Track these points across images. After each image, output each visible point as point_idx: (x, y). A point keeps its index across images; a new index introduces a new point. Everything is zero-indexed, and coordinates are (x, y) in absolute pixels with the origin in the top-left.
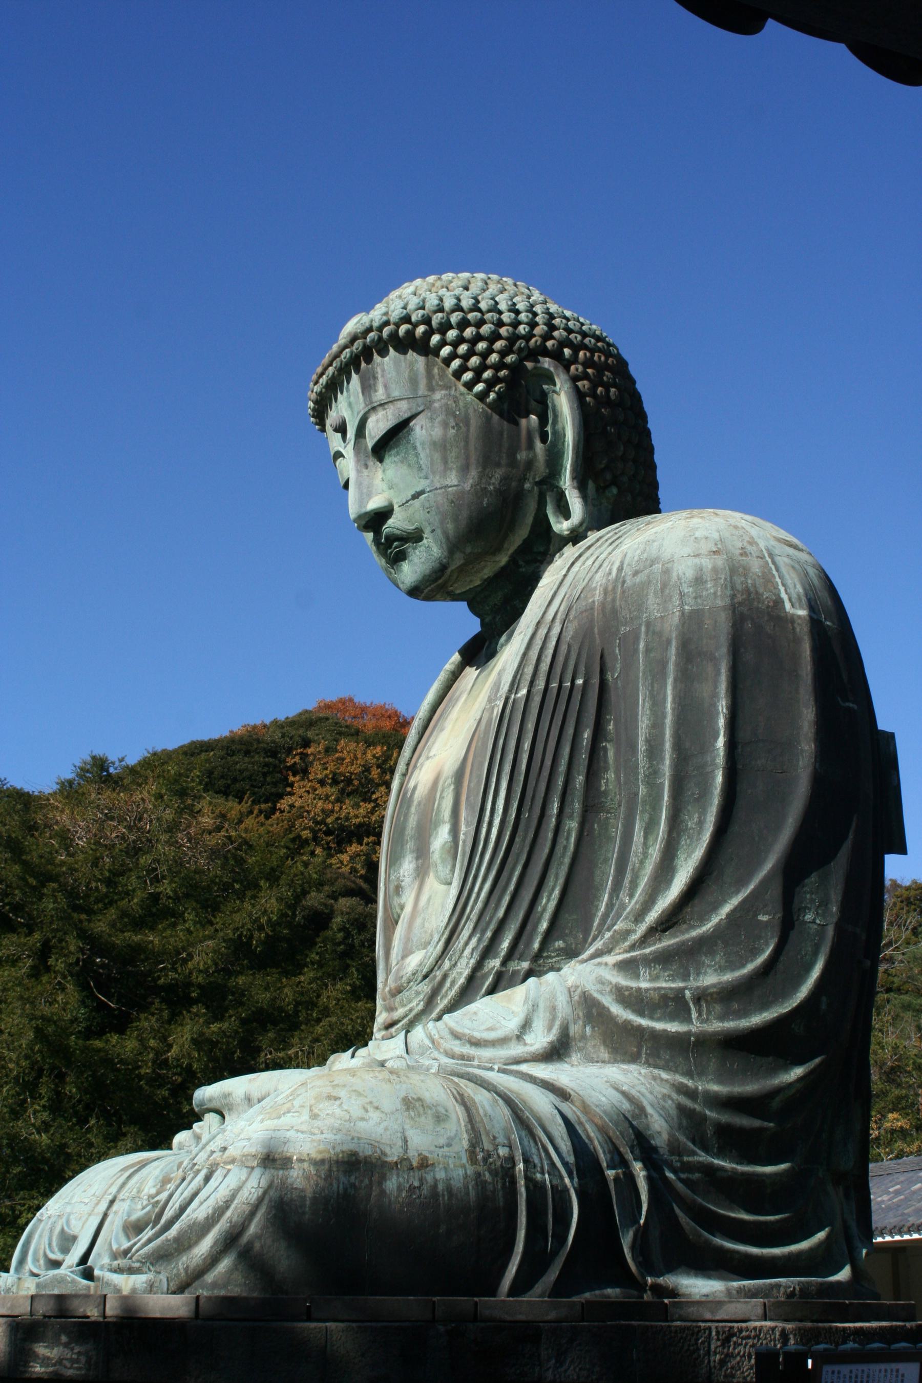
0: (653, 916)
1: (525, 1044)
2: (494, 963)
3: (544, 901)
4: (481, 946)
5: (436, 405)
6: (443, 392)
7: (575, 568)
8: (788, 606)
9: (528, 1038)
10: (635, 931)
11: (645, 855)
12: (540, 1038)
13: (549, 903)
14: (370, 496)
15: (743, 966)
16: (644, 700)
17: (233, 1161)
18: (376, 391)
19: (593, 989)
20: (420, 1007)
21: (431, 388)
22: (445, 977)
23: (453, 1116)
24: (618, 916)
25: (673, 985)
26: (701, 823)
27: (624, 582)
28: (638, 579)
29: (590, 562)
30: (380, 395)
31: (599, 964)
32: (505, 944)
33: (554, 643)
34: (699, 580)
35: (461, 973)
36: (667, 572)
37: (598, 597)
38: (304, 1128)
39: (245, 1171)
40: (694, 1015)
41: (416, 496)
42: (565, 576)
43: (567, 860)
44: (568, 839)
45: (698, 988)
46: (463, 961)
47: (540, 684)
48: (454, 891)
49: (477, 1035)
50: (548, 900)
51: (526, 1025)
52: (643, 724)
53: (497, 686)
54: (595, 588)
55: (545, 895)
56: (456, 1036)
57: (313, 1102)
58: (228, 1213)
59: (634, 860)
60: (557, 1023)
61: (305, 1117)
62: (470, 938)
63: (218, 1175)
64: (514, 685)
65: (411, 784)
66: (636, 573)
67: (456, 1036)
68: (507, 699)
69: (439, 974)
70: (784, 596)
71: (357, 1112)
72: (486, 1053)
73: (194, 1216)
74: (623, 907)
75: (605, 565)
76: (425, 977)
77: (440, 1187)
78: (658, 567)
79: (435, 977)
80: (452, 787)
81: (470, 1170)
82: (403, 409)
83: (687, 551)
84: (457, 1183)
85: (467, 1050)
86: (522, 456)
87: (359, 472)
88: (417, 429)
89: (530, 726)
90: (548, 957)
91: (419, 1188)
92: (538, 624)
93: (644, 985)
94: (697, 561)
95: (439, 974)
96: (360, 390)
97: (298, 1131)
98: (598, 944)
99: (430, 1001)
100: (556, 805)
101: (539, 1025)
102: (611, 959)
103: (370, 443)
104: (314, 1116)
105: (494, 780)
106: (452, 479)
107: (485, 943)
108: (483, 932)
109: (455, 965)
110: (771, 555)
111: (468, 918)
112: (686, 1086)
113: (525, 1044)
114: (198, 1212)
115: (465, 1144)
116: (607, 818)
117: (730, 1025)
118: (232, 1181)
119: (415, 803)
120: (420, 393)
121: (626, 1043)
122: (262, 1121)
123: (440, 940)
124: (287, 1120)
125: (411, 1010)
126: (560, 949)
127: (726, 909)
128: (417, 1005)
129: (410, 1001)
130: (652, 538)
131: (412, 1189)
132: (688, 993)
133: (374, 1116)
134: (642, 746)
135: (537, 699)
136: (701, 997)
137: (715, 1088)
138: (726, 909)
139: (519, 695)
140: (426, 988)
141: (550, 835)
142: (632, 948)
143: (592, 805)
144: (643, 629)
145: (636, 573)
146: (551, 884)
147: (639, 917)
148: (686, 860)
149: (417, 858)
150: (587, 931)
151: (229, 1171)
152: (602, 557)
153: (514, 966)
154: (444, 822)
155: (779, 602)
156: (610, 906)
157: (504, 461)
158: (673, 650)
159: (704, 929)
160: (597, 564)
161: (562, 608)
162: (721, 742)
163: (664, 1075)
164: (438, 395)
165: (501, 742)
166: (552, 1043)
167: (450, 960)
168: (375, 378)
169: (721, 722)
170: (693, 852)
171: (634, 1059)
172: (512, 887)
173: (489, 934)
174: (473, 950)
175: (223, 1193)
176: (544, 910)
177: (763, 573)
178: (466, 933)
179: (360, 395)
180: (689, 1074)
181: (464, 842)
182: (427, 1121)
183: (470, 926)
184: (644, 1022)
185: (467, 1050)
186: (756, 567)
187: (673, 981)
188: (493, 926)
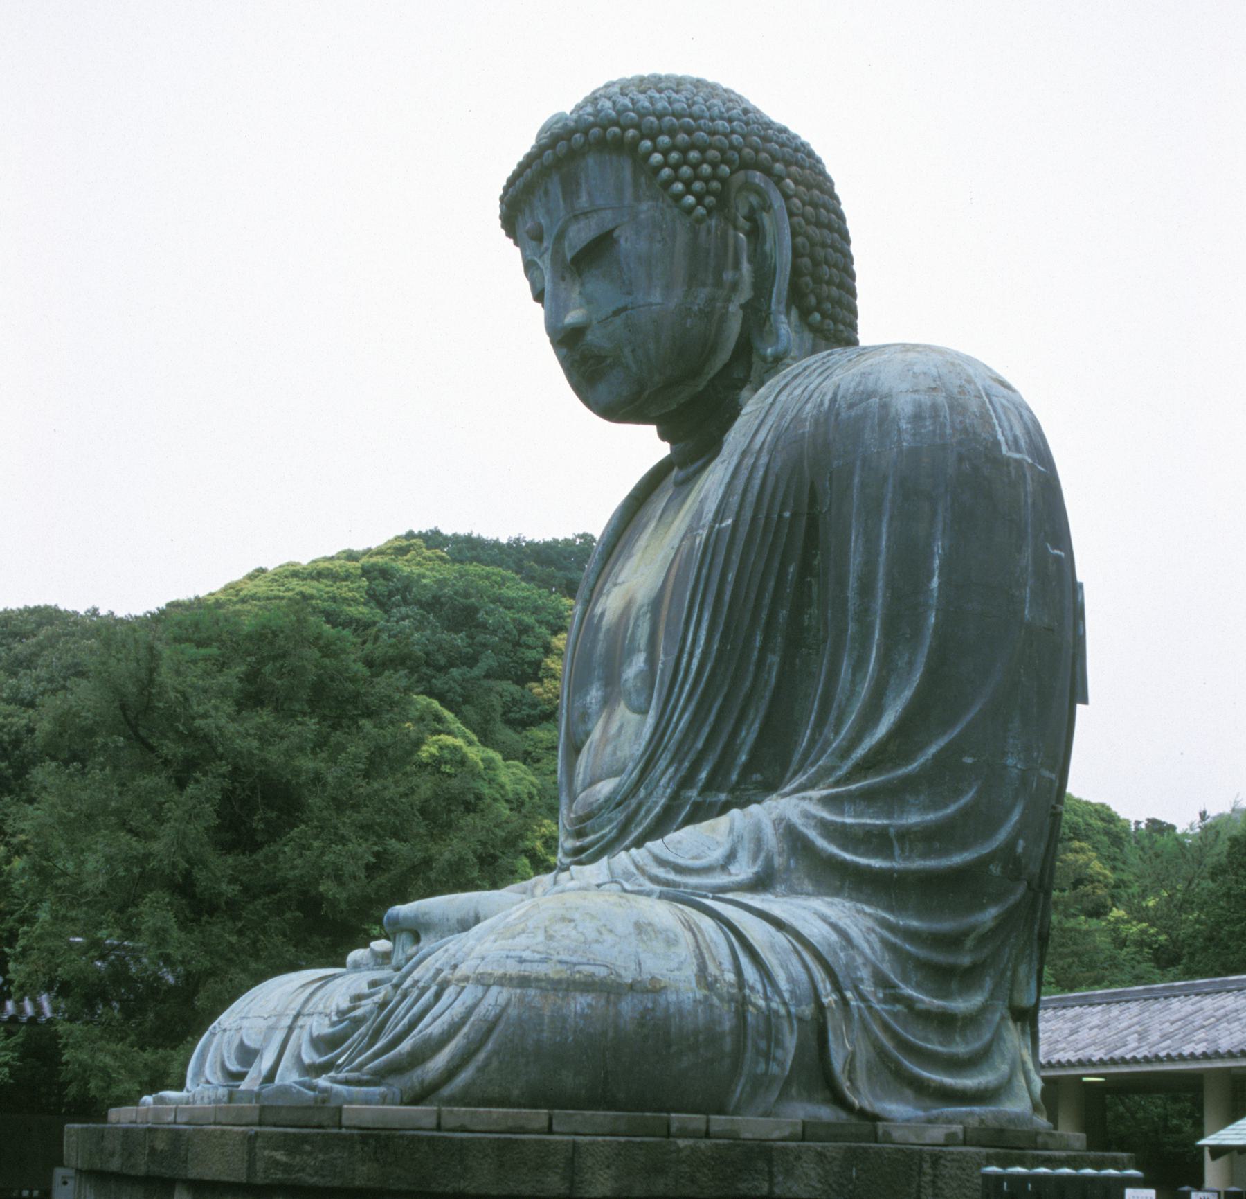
0: (859, 753)
1: (730, 874)
2: (693, 794)
3: (743, 734)
5: (642, 216)
6: (650, 203)
7: (783, 397)
8: (1004, 448)
10: (840, 767)
11: (853, 693)
12: (743, 870)
13: (749, 735)
14: (567, 310)
15: (946, 806)
16: (857, 537)
17: (467, 979)
18: (579, 198)
19: (798, 821)
20: (613, 834)
21: (637, 198)
22: (640, 805)
23: (682, 940)
24: (823, 751)
25: (878, 822)
26: (911, 663)
27: (838, 414)
28: (853, 413)
29: (798, 392)
30: (583, 201)
31: (804, 798)
32: (703, 775)
33: (761, 473)
34: (917, 417)
35: (656, 803)
36: (884, 406)
37: (808, 427)
38: (540, 948)
39: (480, 989)
40: (897, 852)
41: (616, 313)
42: (772, 404)
43: (768, 694)
44: (769, 672)
45: (902, 826)
46: (660, 791)
47: (748, 514)
48: (651, 719)
49: (681, 861)
50: (748, 734)
51: (731, 857)
52: (855, 562)
53: (698, 515)
54: (806, 419)
55: (745, 728)
56: (661, 862)
57: (547, 923)
58: (465, 1029)
59: (840, 695)
60: (762, 855)
61: (541, 937)
62: (667, 768)
63: (450, 991)
64: (719, 515)
65: (598, 610)
66: (851, 406)
67: (661, 862)
68: (712, 528)
69: (634, 803)
70: (1000, 437)
71: (592, 935)
72: (693, 880)
73: (429, 1031)
74: (828, 743)
75: (815, 395)
76: (618, 805)
77: (672, 1009)
78: (874, 401)
79: (629, 805)
80: (648, 616)
81: (700, 994)
82: (607, 219)
83: (904, 386)
84: (688, 1006)
85: (672, 876)
86: (728, 276)
87: (555, 284)
88: (622, 241)
89: (736, 558)
90: (746, 790)
91: (653, 1009)
92: (744, 454)
93: (849, 820)
94: (916, 396)
95: (634, 803)
96: (560, 195)
97: (534, 951)
98: (800, 779)
99: (624, 830)
101: (743, 856)
102: (816, 794)
104: (550, 938)
105: (696, 610)
106: (656, 297)
107: (683, 772)
108: (681, 762)
109: (650, 794)
110: (988, 395)
111: (665, 748)
112: (888, 920)
113: (730, 874)
114: (432, 1026)
115: (695, 968)
116: (809, 654)
117: (931, 863)
118: (467, 997)
119: (603, 630)
120: (626, 203)
121: (835, 877)
122: (495, 941)
123: (635, 768)
125: (603, 837)
126: (756, 782)
127: (932, 750)
128: (609, 831)
129: (602, 828)
130: (869, 370)
131: (646, 1009)
132: (892, 830)
133: (609, 938)
134: (852, 582)
135: (743, 530)
136: (905, 835)
137: (915, 924)
138: (932, 750)
139: (724, 525)
140: (620, 816)
141: (752, 668)
142: (837, 783)
143: (797, 641)
144: (858, 463)
145: (851, 406)
146: (751, 717)
147: (845, 753)
148: (894, 699)
149: (606, 685)
150: (785, 767)
151: (463, 988)
152: (812, 387)
153: (711, 798)
154: (639, 651)
155: (997, 444)
156: (813, 741)
157: (710, 280)
158: (890, 488)
159: (910, 768)
160: (806, 394)
161: (769, 438)
162: (935, 583)
163: (868, 909)
164: (644, 206)
165: (704, 572)
166: (757, 873)
167: (646, 788)
168: (578, 184)
169: (937, 562)
170: (902, 691)
171: (837, 892)
172: (712, 718)
173: (687, 764)
174: (670, 779)
175: (458, 1009)
176: (743, 742)
177: (981, 413)
178: (662, 763)
179: (561, 202)
180: (889, 909)
181: (663, 671)
182: (659, 946)
183: (667, 756)
184: (848, 857)
185: (672, 876)
186: (974, 406)
187: (877, 818)
188: (691, 756)
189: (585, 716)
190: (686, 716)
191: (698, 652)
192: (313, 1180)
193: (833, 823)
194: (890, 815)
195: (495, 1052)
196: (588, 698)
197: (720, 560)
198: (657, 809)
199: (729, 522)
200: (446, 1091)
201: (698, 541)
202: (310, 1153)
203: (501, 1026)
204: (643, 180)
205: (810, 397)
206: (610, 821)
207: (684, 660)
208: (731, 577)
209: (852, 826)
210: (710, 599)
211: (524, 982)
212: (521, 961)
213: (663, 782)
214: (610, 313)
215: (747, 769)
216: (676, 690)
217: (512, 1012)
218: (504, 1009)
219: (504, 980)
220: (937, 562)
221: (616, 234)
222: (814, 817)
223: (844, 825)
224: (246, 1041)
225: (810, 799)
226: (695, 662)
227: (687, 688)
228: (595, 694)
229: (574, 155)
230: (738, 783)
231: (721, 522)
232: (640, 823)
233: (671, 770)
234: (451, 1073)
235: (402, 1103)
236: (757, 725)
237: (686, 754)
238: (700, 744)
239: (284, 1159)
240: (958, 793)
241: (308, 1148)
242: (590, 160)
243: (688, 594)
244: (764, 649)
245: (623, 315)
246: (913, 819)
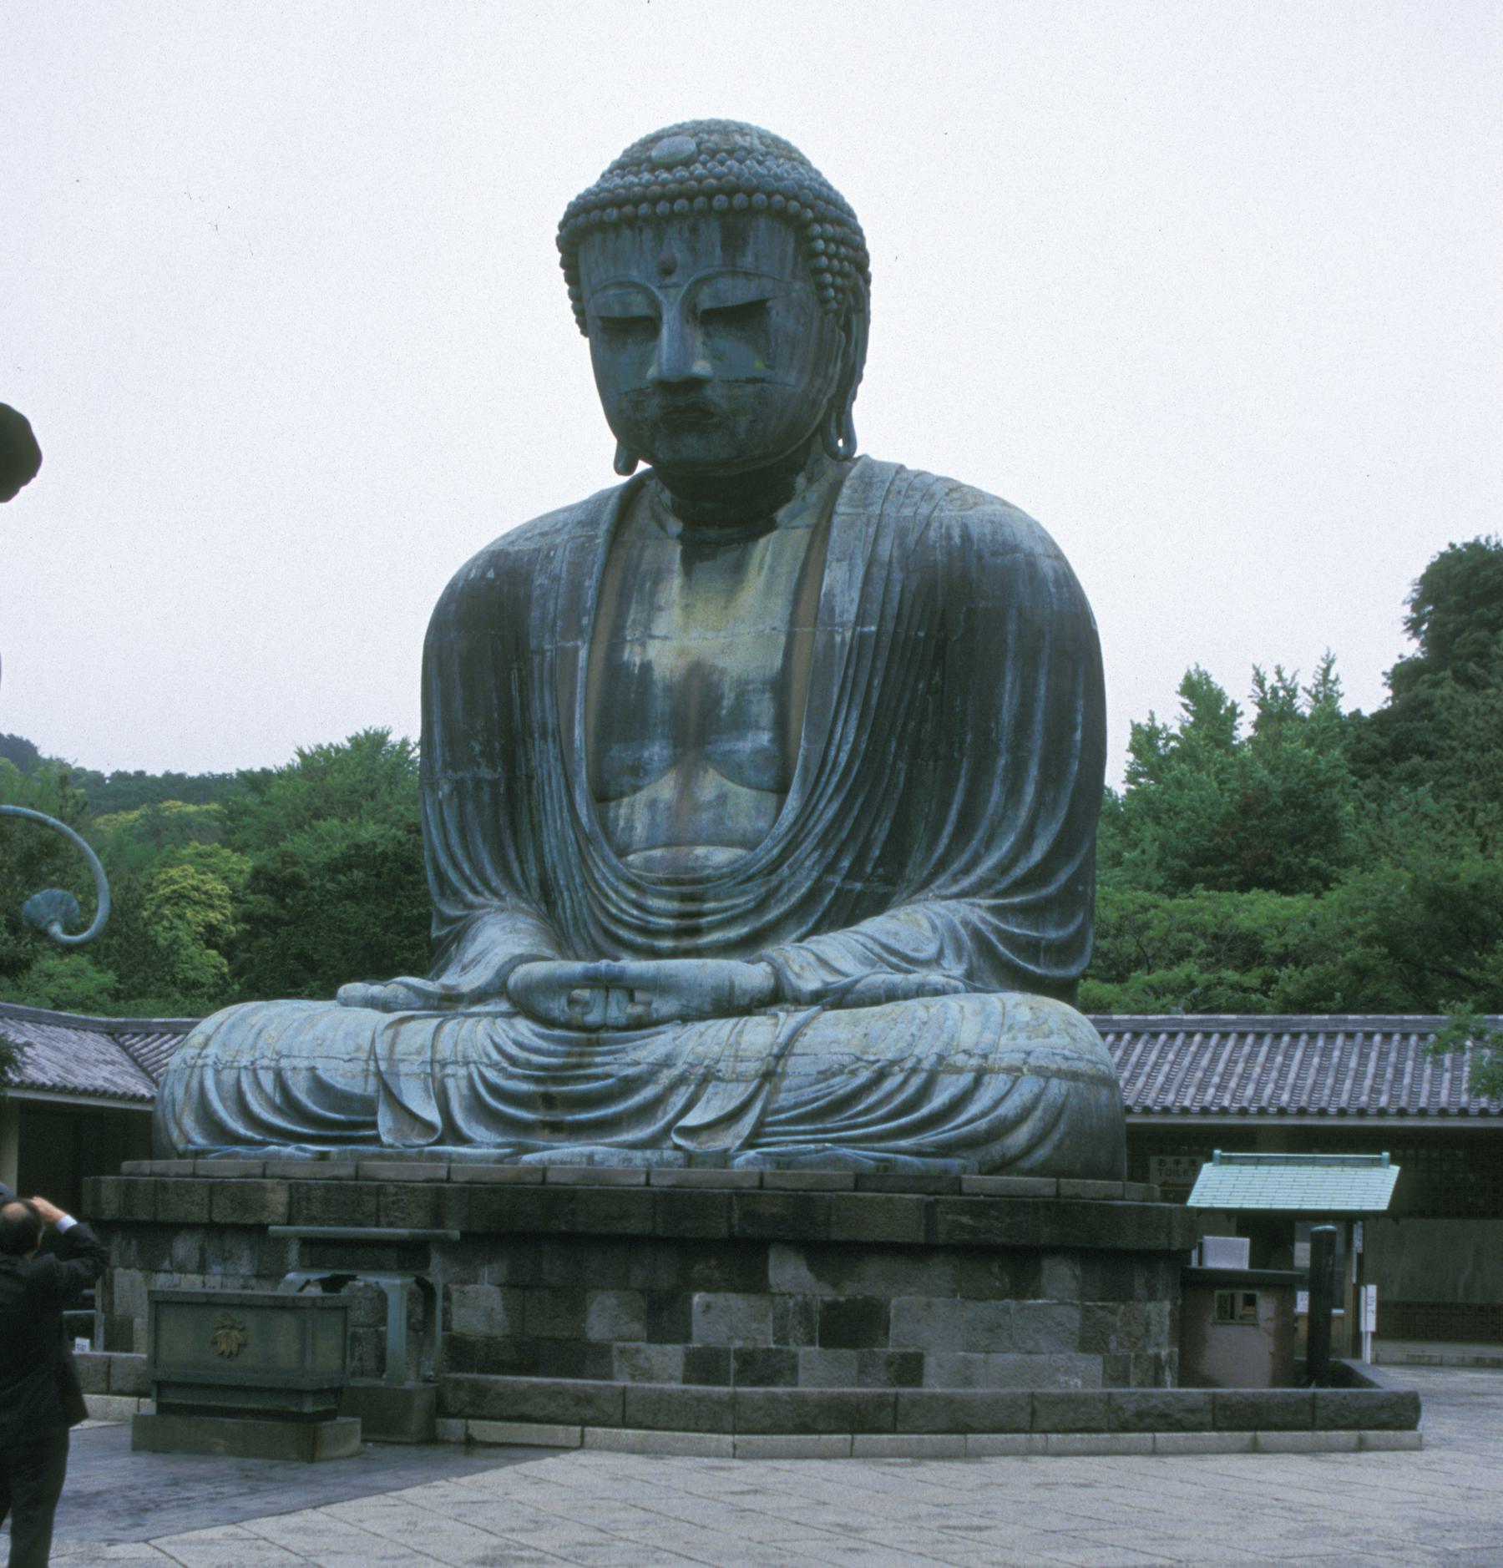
0: (1019, 871)
2: (837, 880)
4: (825, 861)
5: (794, 295)
9: (945, 963)
13: (882, 832)
22: (781, 884)
26: (1055, 801)
27: (980, 558)
30: (748, 261)
32: (845, 864)
35: (799, 884)
36: (1032, 564)
39: (1042, 1081)
40: (1042, 960)
41: (752, 381)
51: (941, 954)
58: (1038, 1113)
61: (1068, 1040)
64: (861, 619)
69: (774, 880)
76: (749, 879)
79: (768, 882)
88: (773, 313)
92: (870, 563)
96: (718, 243)
100: (894, 744)
101: (949, 952)
103: (706, 301)
104: (1073, 1039)
108: (826, 848)
109: (793, 874)
124: (1054, 1039)
125: (733, 907)
135: (886, 640)
140: (757, 890)
141: (888, 771)
142: (997, 895)
145: (994, 553)
149: (675, 746)
151: (1017, 1078)
154: (758, 728)
162: (1078, 736)
164: (798, 285)
165: (851, 671)
169: (1079, 718)
173: (832, 851)
176: (876, 838)
179: (718, 250)
181: (806, 758)
189: (638, 772)
190: (835, 806)
191: (847, 747)
192: (999, 1240)
193: (1005, 931)
194: (1036, 927)
195: (1067, 1134)
196: (646, 754)
197: (867, 663)
198: (803, 890)
199: (873, 628)
200: (1025, 1164)
201: (838, 639)
202: (997, 1218)
203: (1067, 1113)
204: (800, 259)
205: (928, 525)
206: (744, 893)
207: (833, 753)
208: (876, 682)
209: (1019, 935)
210: (858, 700)
211: (1074, 1076)
212: (1066, 1058)
213: (808, 864)
214: (744, 377)
215: (880, 862)
216: (824, 779)
217: (1073, 1100)
218: (1068, 1095)
219: (1060, 1074)
220: (1079, 718)
221: (769, 304)
222: (990, 924)
223: (1013, 934)
224: (325, 1076)
225: (979, 906)
226: (844, 757)
227: (835, 779)
228: (656, 751)
229: (750, 211)
230: (872, 874)
231: (863, 625)
232: (782, 900)
233: (816, 855)
234: (1029, 1149)
235: (980, 1173)
236: (887, 824)
237: (833, 839)
238: (844, 834)
239: (970, 1222)
240: (1073, 915)
241: (993, 1213)
242: (762, 223)
243: (836, 690)
244: (897, 756)
245: (758, 386)
246: (1053, 934)
